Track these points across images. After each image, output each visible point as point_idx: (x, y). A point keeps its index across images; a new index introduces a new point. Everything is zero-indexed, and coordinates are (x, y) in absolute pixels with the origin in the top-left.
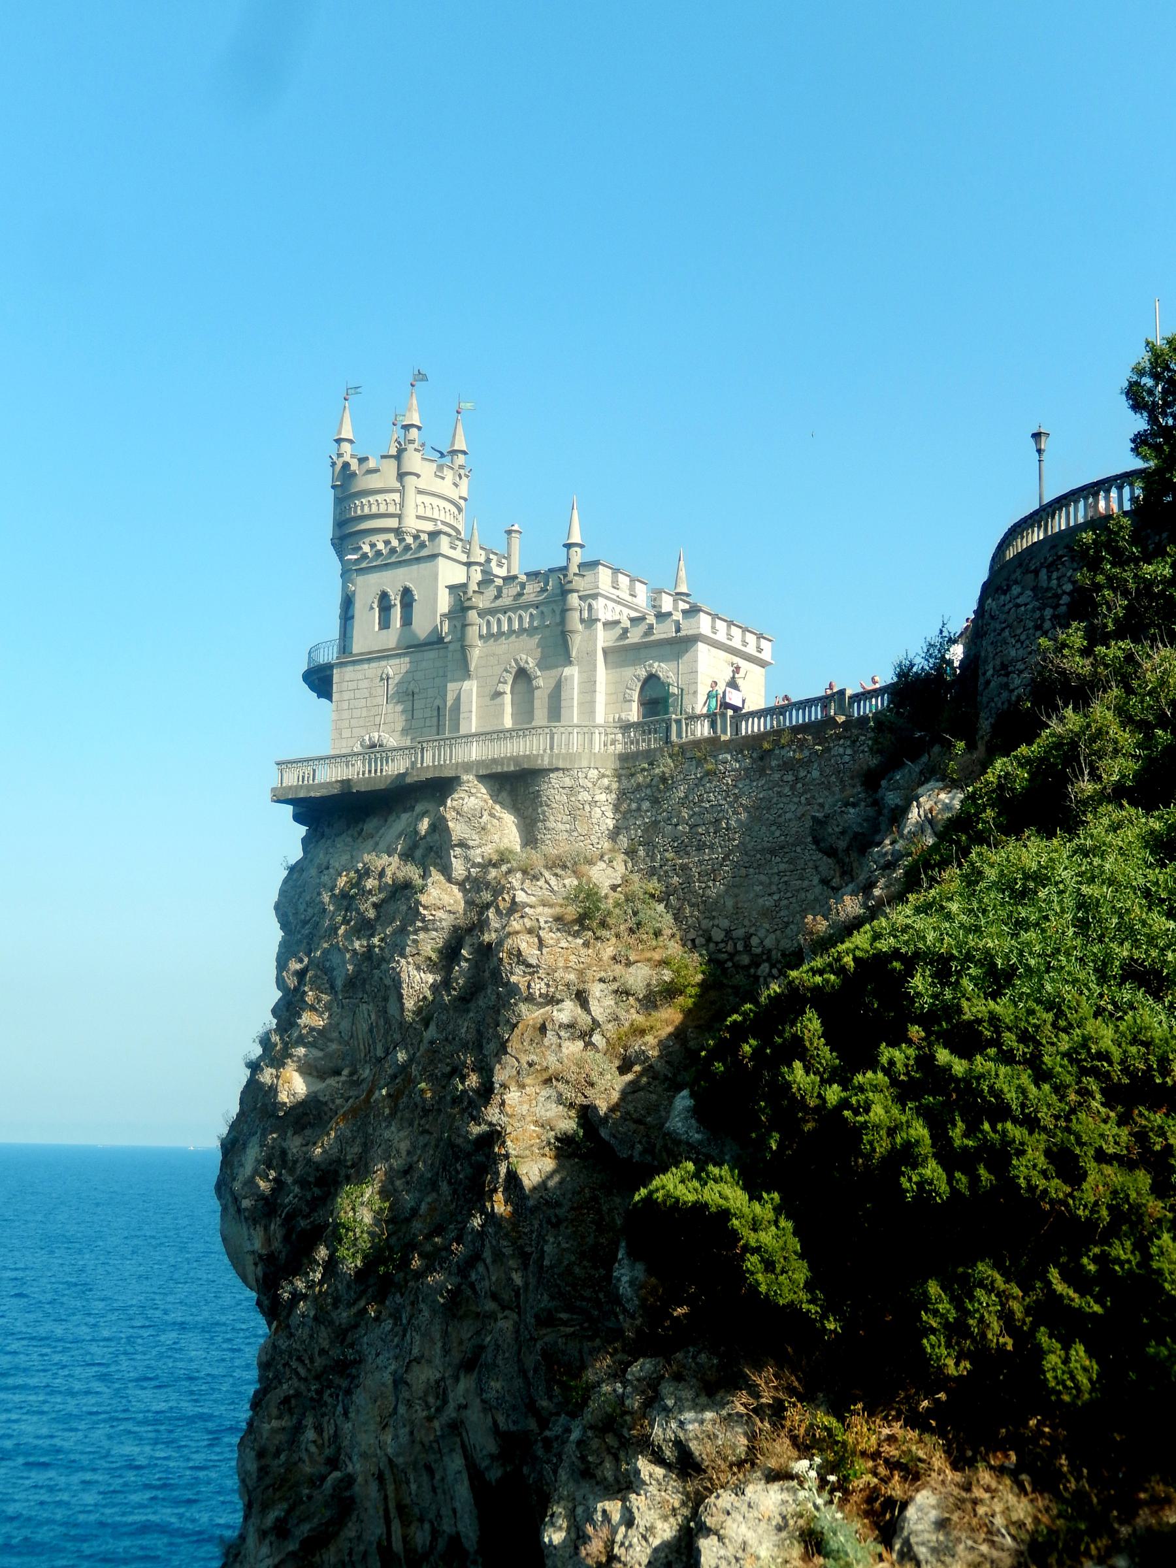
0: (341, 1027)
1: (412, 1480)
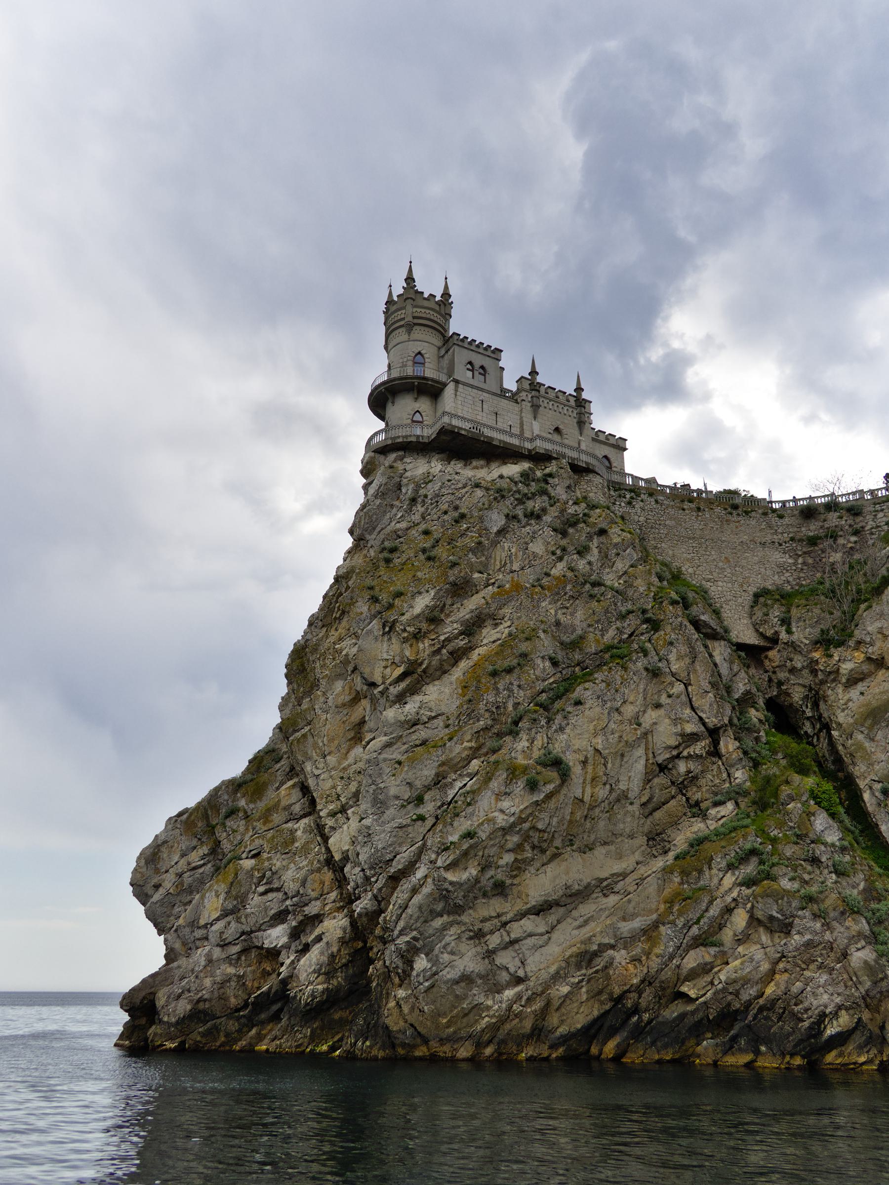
1: (610, 762)
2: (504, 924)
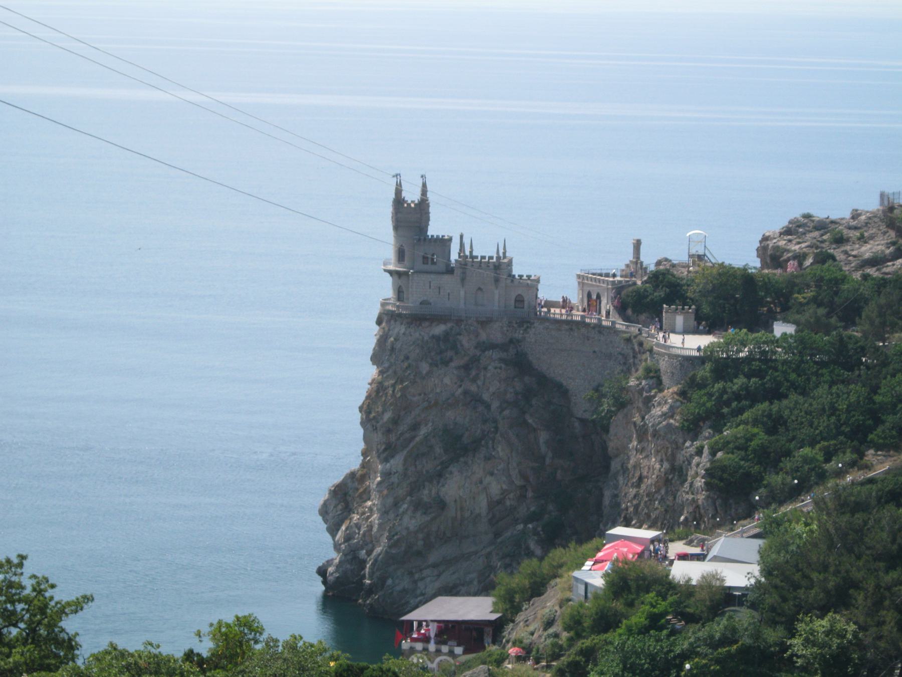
2: (421, 570)
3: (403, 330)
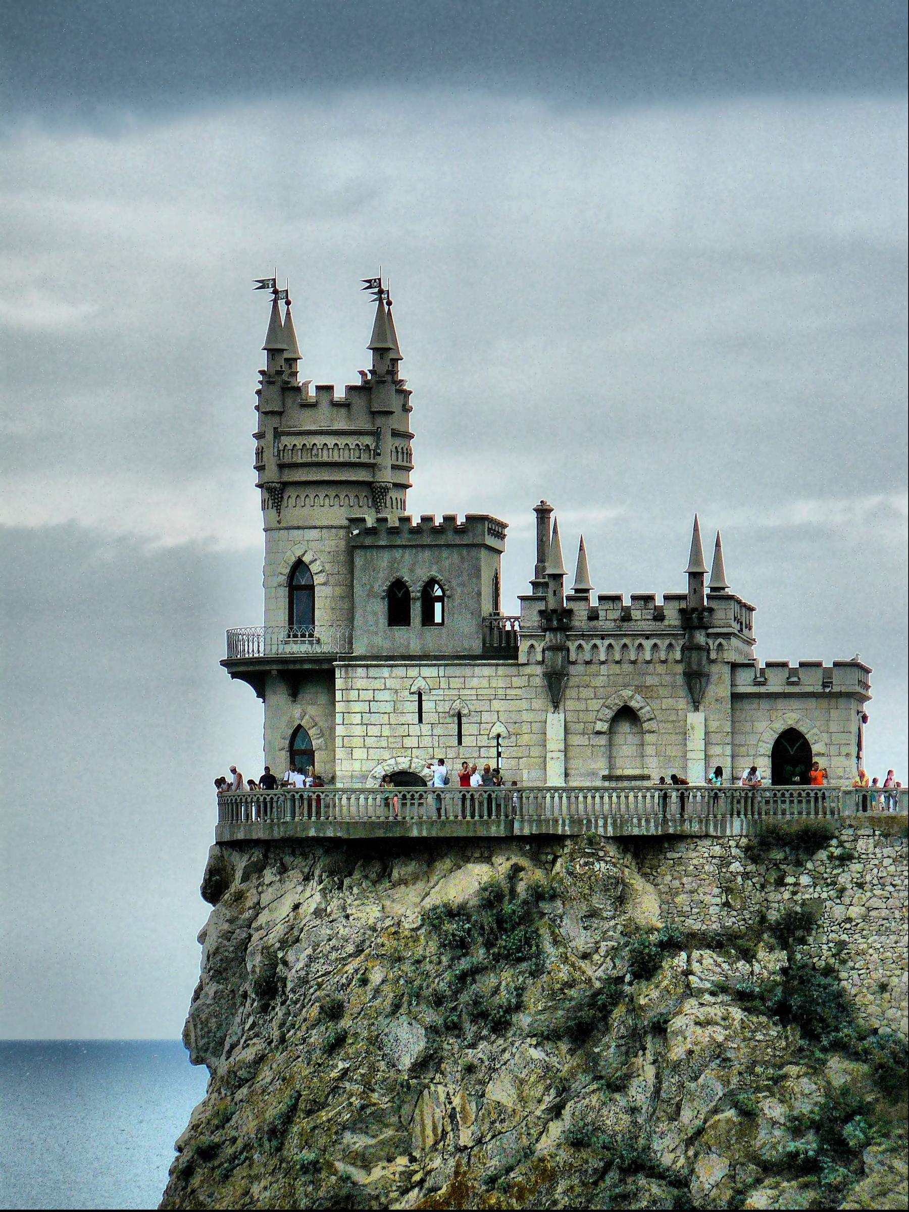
0: (403, 1112)
3: (309, 907)
